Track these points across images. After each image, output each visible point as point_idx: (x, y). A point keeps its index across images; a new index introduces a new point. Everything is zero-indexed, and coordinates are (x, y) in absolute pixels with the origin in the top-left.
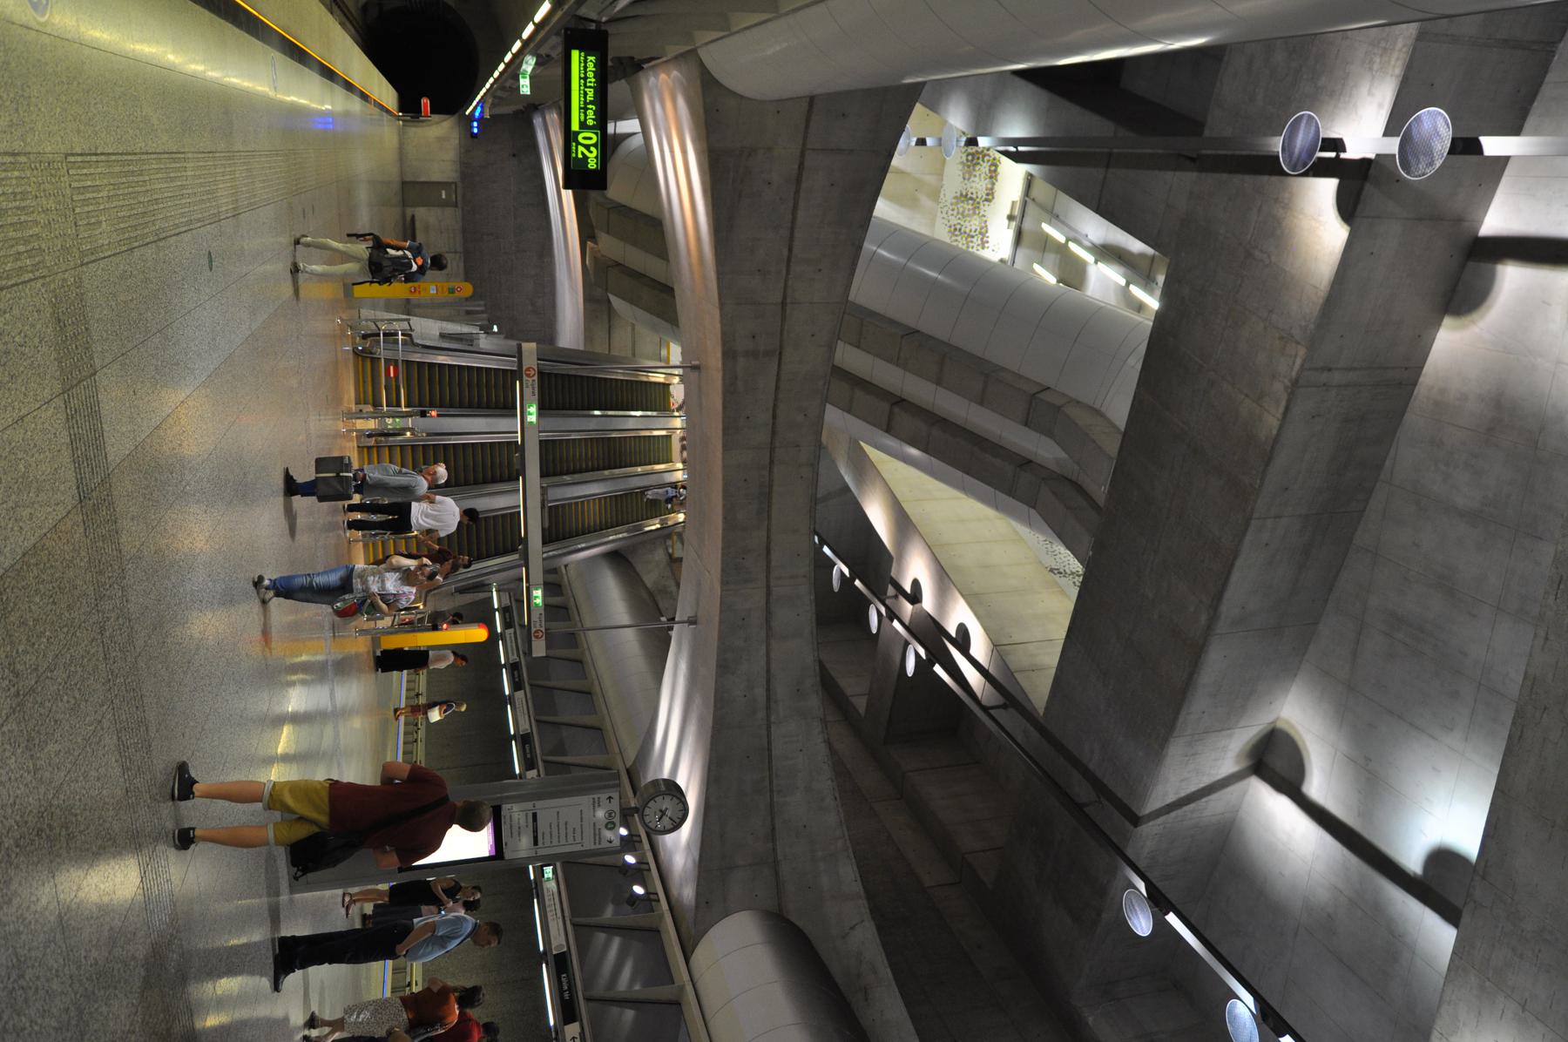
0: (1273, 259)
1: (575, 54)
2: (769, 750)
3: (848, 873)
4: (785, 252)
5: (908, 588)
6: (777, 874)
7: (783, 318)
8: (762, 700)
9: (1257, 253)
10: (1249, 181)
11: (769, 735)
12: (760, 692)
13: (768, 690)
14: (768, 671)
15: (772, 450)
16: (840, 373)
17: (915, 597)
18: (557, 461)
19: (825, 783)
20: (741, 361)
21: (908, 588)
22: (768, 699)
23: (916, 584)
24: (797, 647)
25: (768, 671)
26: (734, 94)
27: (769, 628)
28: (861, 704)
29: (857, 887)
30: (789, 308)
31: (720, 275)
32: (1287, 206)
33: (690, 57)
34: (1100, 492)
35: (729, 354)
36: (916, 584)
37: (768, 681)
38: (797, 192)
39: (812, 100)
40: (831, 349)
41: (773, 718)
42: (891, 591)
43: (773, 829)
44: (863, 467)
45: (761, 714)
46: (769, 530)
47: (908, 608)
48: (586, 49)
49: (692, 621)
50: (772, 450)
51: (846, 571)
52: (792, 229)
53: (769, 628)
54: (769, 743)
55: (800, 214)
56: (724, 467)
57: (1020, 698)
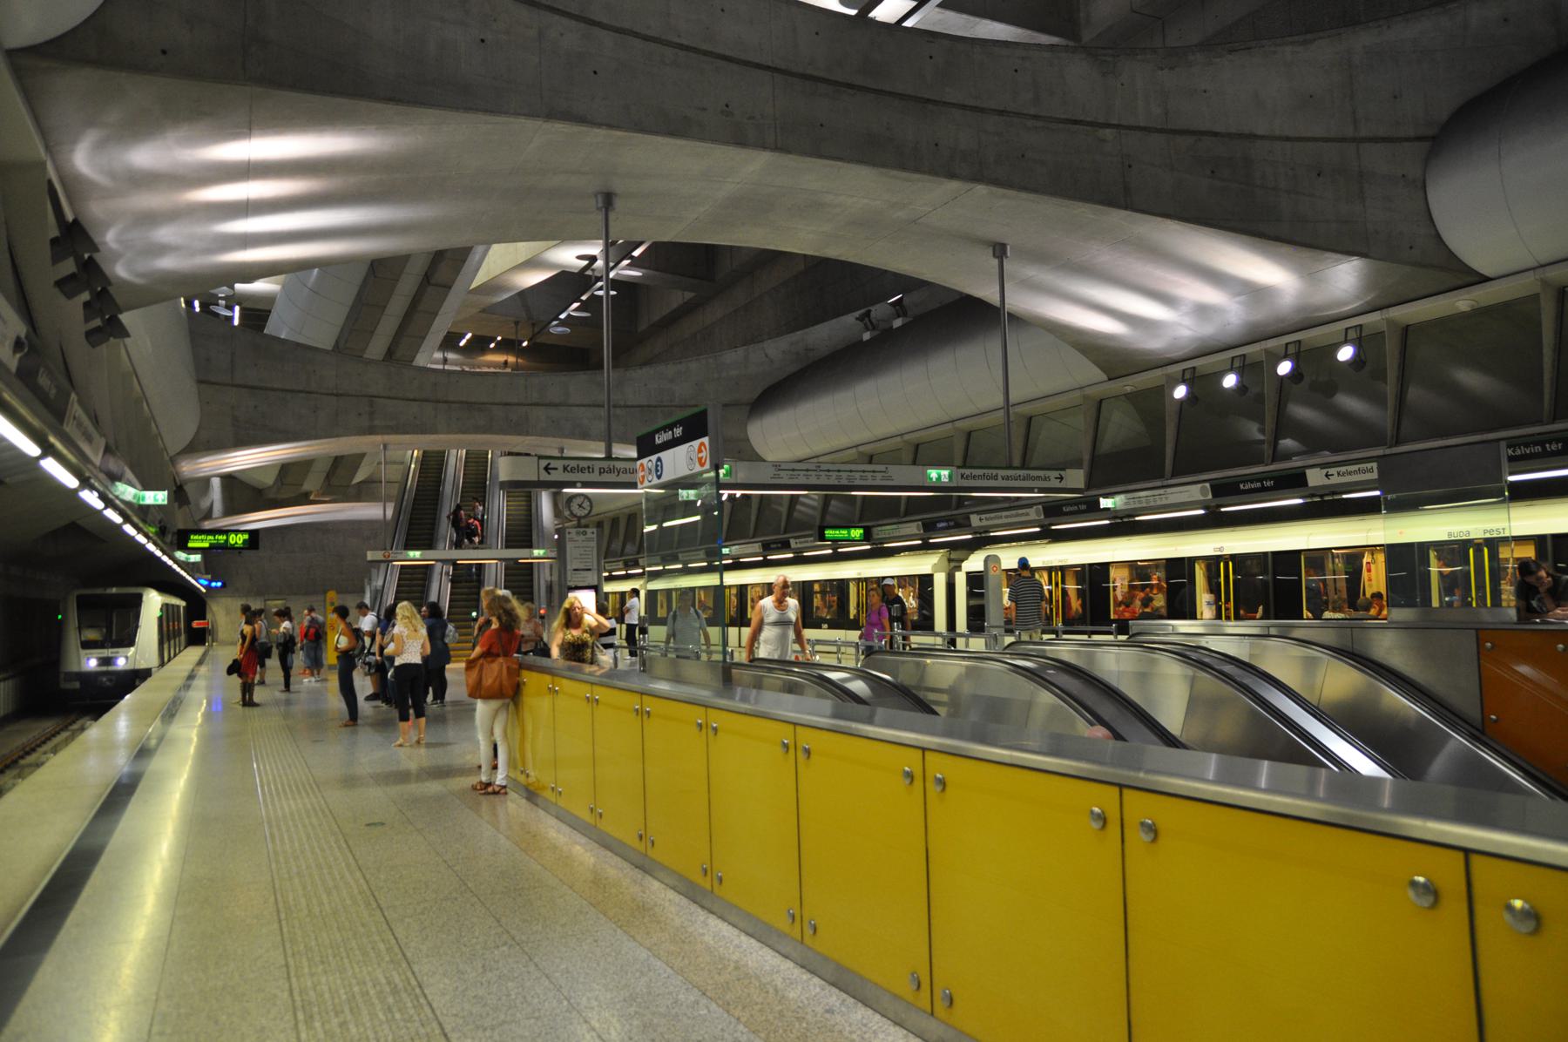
1: (190, 545)
3: (732, 357)
5: (585, 263)
15: (438, 402)
16: (390, 354)
17: (593, 259)
18: (466, 533)
19: (670, 369)
20: (377, 422)
21: (585, 263)
23: (580, 257)
24: (576, 385)
26: (197, 433)
28: (689, 295)
29: (741, 351)
31: (316, 438)
33: (173, 460)
35: (371, 431)
36: (580, 257)
39: (200, 382)
40: (371, 361)
42: (589, 273)
44: (491, 287)
47: (600, 263)
48: (187, 540)
50: (438, 402)
51: (576, 305)
56: (449, 432)
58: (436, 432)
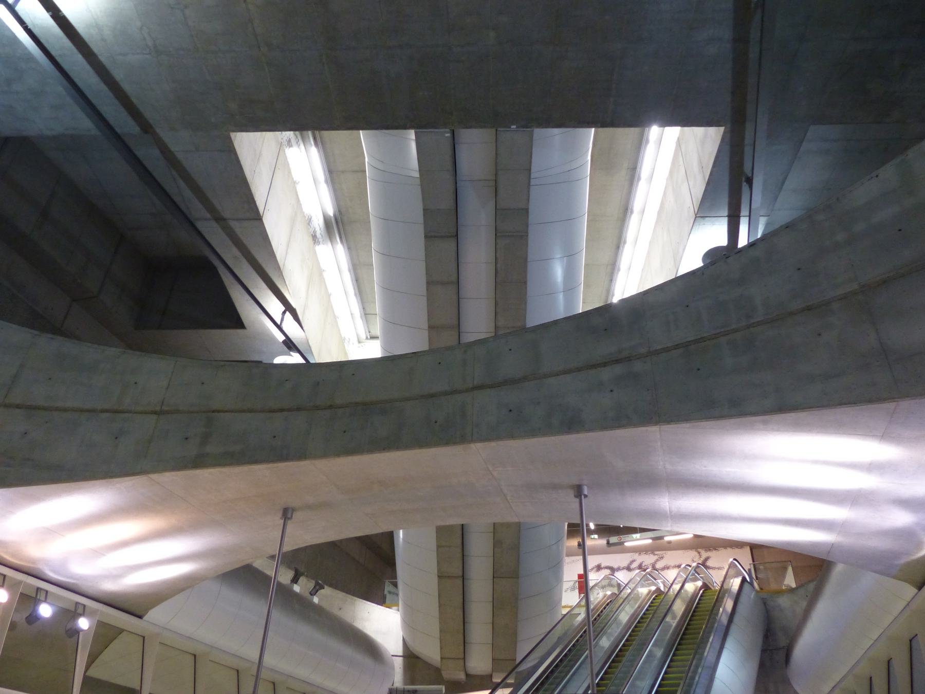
0: (139, 24)
2: (686, 345)
4: (104, 416)
6: (885, 282)
7: (177, 411)
8: (618, 369)
9: (150, 44)
10: (118, 74)
11: (667, 350)
12: (606, 374)
13: (605, 365)
14: (579, 369)
15: (318, 408)
22: (617, 361)
25: (579, 369)
27: (525, 378)
29: (889, 173)
30: (165, 408)
32: (98, 26)
34: (475, 147)
35: (199, 462)
37: (594, 366)
38: (46, 409)
41: (643, 350)
43: (809, 309)
45: (638, 366)
46: (407, 399)
49: (578, 492)
52: (82, 411)
53: (525, 378)
54: (677, 347)
55: (69, 404)
57: (726, 163)
58: (302, 455)
